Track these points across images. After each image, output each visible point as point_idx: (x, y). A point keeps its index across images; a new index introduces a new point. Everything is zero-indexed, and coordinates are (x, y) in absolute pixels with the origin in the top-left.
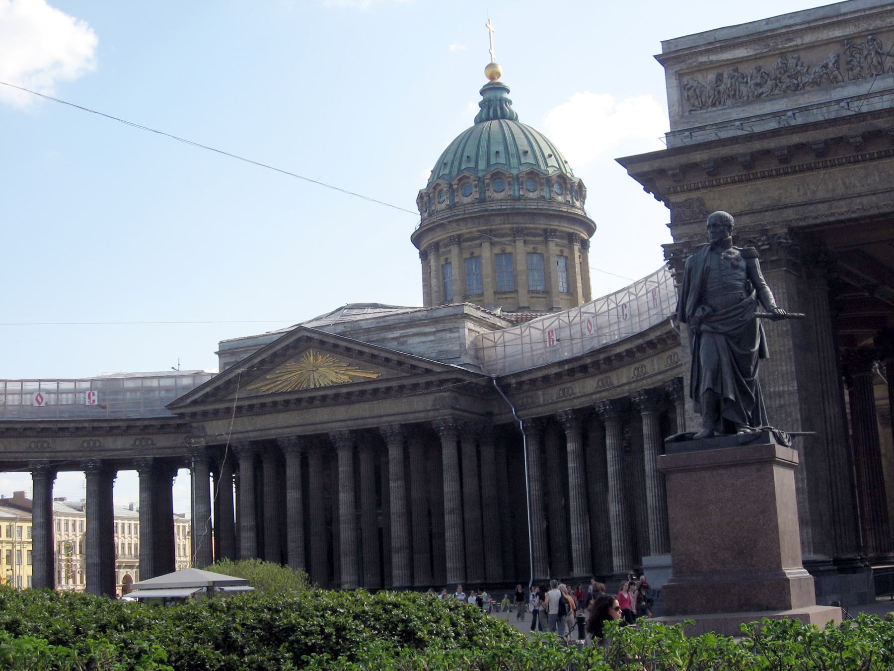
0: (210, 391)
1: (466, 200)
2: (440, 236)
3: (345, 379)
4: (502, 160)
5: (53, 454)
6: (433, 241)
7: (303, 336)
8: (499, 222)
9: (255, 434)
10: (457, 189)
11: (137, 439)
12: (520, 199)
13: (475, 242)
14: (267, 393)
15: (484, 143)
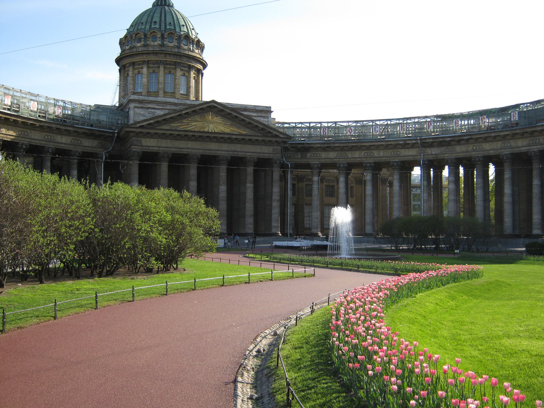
0: (153, 122)
3: (227, 130)
5: (30, 140)
6: (147, 59)
7: (213, 105)
8: (185, 60)
9: (175, 149)
10: (166, 38)
11: (74, 139)
13: (172, 66)
14: (181, 129)
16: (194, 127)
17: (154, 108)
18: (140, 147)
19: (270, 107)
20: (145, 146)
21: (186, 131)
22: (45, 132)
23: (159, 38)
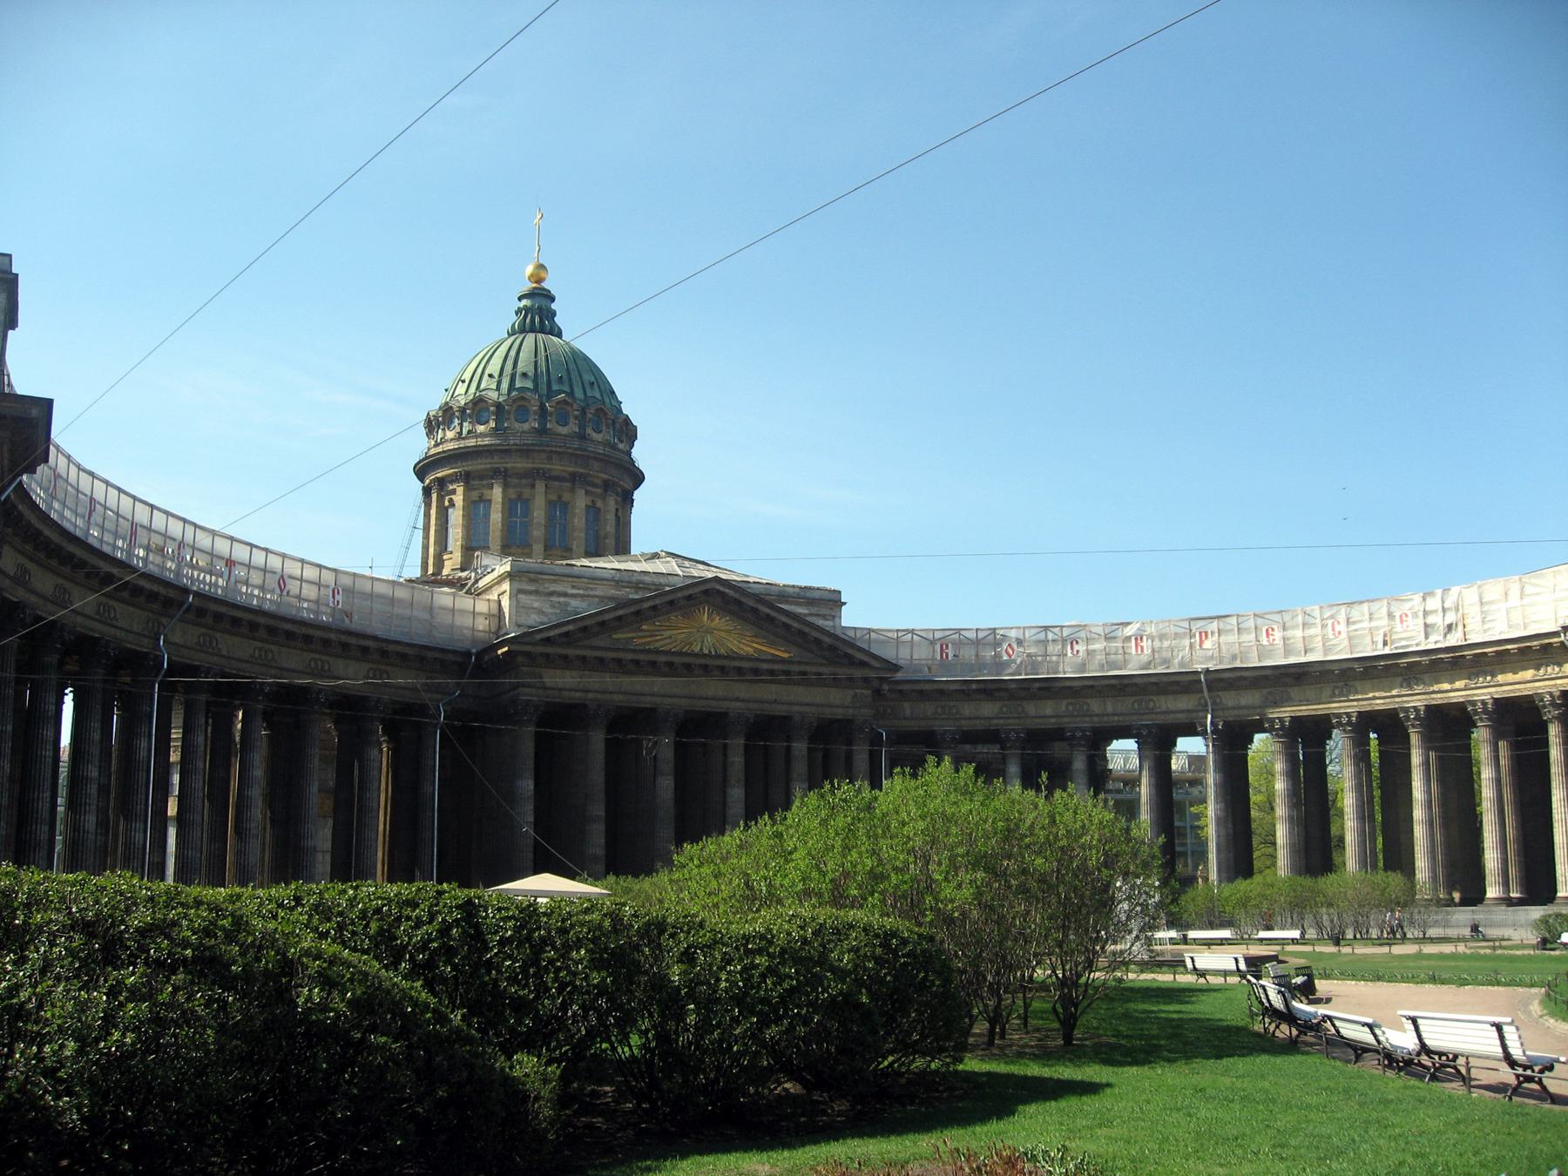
1: (564, 430)
2: (520, 464)
4: (598, 395)
7: (714, 589)
9: (621, 697)
12: (614, 447)
15: (572, 366)
16: (666, 641)
17: (565, 595)
18: (541, 692)
19: (840, 592)
20: (553, 689)
21: (649, 651)
22: (312, 651)
23: (535, 413)
